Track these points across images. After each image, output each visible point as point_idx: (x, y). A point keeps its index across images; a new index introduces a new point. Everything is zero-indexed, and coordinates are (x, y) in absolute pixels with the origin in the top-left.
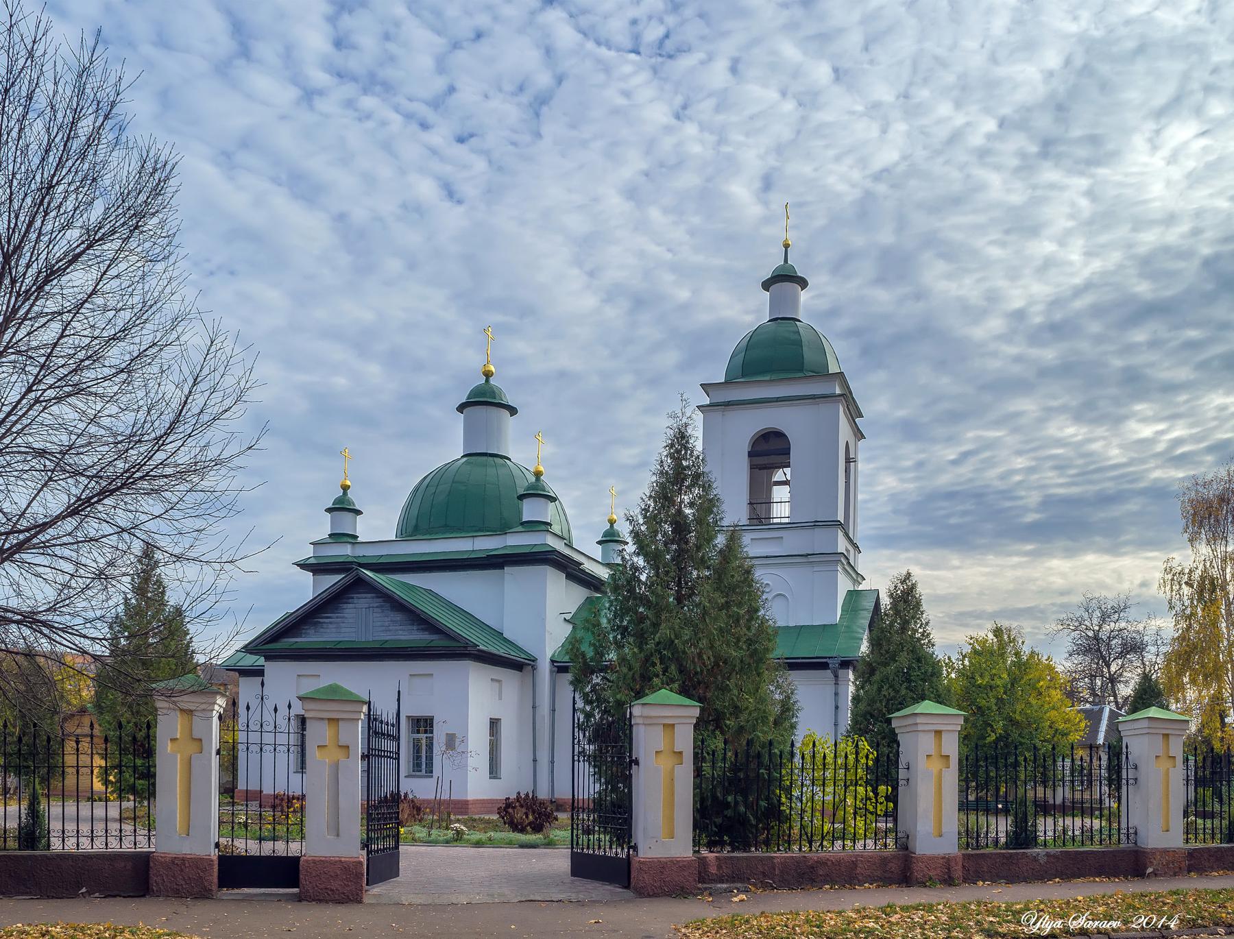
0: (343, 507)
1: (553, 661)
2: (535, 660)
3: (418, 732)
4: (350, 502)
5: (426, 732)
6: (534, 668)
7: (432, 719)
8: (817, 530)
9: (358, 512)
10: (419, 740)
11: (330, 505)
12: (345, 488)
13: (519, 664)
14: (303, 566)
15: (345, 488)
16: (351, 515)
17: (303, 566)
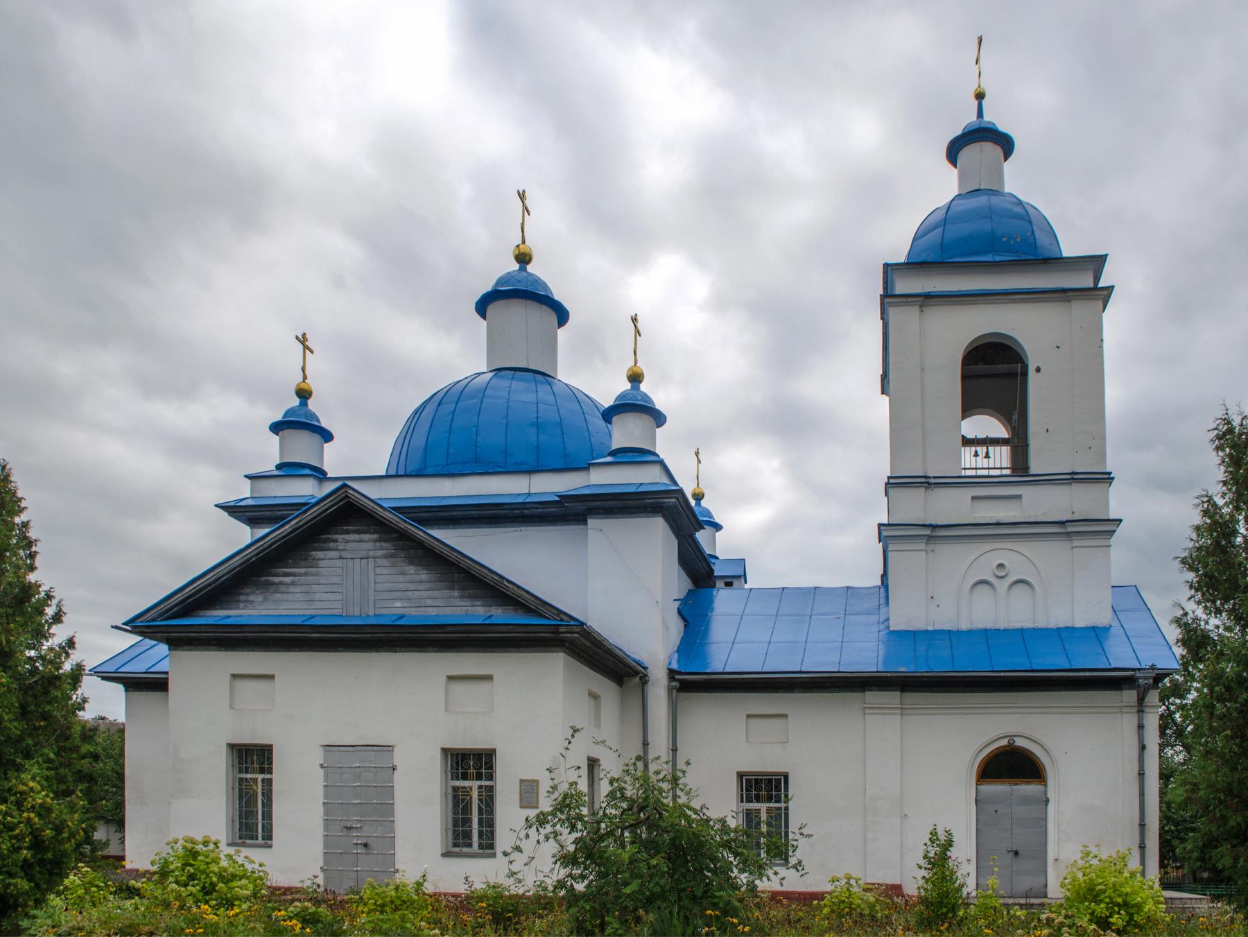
1: (672, 673)
3: (465, 777)
5: (479, 777)
6: (644, 680)
10: (467, 791)
13: (619, 670)
16: (316, 438)
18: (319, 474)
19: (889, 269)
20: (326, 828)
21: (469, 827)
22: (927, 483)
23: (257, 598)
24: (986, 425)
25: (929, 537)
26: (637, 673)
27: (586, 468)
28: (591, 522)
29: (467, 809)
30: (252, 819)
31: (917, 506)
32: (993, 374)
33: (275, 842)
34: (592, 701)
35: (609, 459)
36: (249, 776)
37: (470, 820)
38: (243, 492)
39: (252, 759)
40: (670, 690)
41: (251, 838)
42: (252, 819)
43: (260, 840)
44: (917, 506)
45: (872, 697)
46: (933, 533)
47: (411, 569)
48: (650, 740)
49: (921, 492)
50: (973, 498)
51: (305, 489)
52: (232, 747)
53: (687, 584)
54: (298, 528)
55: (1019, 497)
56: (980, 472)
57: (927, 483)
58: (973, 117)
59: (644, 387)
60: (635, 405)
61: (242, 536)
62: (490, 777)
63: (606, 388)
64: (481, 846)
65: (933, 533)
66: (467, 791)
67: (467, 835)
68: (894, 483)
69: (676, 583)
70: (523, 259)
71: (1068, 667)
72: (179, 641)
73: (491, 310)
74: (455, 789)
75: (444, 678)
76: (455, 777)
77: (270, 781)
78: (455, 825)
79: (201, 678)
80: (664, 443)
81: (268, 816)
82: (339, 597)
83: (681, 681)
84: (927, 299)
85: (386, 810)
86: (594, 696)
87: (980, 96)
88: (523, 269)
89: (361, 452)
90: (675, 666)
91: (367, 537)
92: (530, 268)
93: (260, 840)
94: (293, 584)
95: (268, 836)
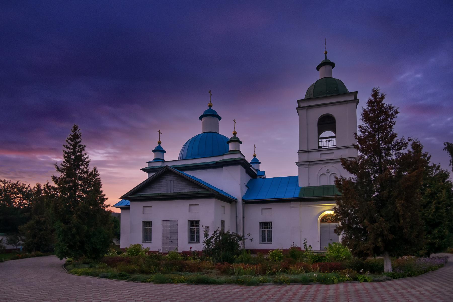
1: (243, 200)
2: (237, 199)
3: (193, 226)
5: (196, 226)
7: (199, 221)
10: (194, 229)
13: (230, 200)
18: (163, 161)
20: (163, 238)
21: (193, 237)
22: (308, 151)
25: (309, 165)
27: (223, 155)
29: (194, 233)
30: (147, 237)
31: (305, 157)
34: (223, 208)
37: (194, 235)
38: (146, 165)
39: (147, 224)
40: (243, 204)
42: (147, 237)
45: (293, 203)
46: (310, 163)
47: (181, 182)
48: (238, 215)
50: (321, 154)
51: (159, 164)
52: (143, 222)
55: (333, 153)
58: (324, 59)
59: (236, 136)
61: (145, 176)
62: (199, 226)
65: (310, 163)
66: (194, 229)
67: (194, 239)
69: (248, 178)
72: (132, 200)
74: (191, 229)
77: (151, 229)
78: (191, 236)
81: (151, 236)
84: (309, 107)
87: (326, 53)
88: (210, 108)
95: (151, 240)
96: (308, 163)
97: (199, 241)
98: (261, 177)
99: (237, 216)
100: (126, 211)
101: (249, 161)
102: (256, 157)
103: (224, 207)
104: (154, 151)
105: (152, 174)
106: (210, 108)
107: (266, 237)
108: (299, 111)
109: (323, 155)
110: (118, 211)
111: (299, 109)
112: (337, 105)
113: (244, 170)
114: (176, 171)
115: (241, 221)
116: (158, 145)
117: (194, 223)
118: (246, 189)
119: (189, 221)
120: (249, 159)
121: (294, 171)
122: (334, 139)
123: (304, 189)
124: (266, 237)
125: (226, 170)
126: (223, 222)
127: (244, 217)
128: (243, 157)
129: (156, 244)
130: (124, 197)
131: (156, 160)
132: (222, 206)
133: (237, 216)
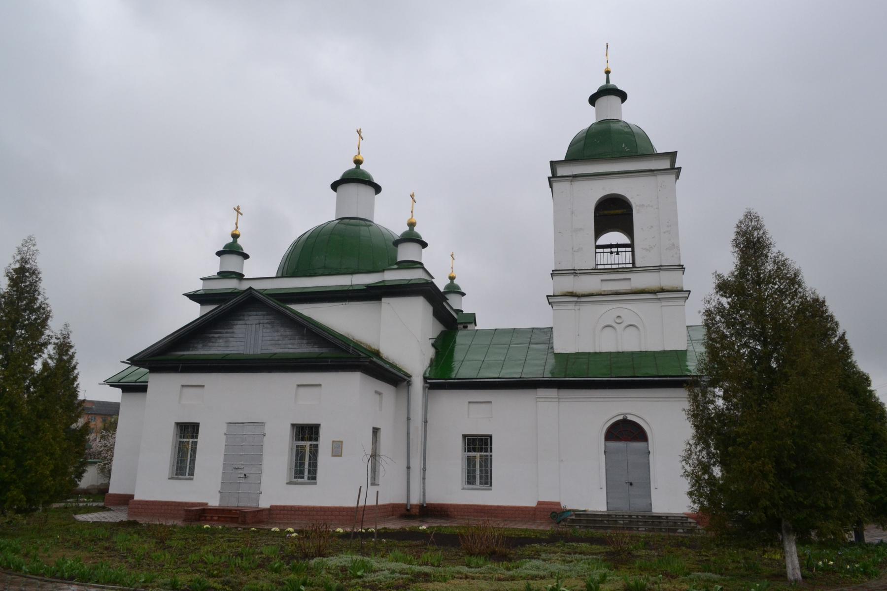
0: (232, 250)
1: (425, 379)
2: (410, 376)
3: (303, 440)
4: (240, 247)
5: (310, 440)
6: (409, 384)
8: (662, 273)
9: (246, 256)
10: (303, 447)
11: (221, 249)
12: (235, 236)
14: (194, 297)
15: (235, 236)
16: (240, 258)
17: (194, 297)
18: (240, 276)
19: (553, 164)
20: (224, 469)
21: (304, 467)
22: (575, 272)
23: (201, 346)
24: (615, 237)
26: (405, 380)
27: (383, 271)
28: (383, 299)
32: (614, 214)
33: (195, 477)
34: (377, 396)
35: (396, 266)
36: (185, 440)
38: (198, 286)
40: (424, 388)
41: (182, 474)
43: (187, 476)
44: (569, 284)
49: (572, 277)
51: (230, 284)
52: (177, 424)
53: (439, 328)
54: (226, 303)
56: (606, 267)
57: (575, 272)
60: (412, 238)
61: (194, 312)
63: (399, 229)
64: (309, 479)
66: (303, 447)
68: (555, 273)
70: (358, 162)
71: (655, 373)
73: (340, 189)
75: (295, 386)
76: (297, 439)
77: (196, 443)
79: (164, 387)
80: (426, 257)
82: (243, 344)
83: (430, 383)
85: (258, 458)
86: (378, 393)
89: (262, 268)
90: (427, 375)
91: (260, 313)
92: (362, 167)
93: (187, 476)
94: (219, 338)
95: (192, 473)
96: (575, 299)
97: (315, 478)
98: (466, 327)
99: (409, 419)
100: (135, 398)
101: (442, 289)
102: (455, 281)
103: (380, 394)
104: (219, 254)
105: (209, 308)
106: (358, 167)
107: (478, 472)
108: (554, 185)
109: (604, 283)
110: (115, 395)
111: (553, 179)
112: (631, 177)
113: (430, 309)
114: (272, 302)
115: (420, 432)
116: (231, 240)
117: (307, 433)
118: (431, 352)
119: (293, 425)
120: (441, 284)
121: (538, 316)
122: (630, 249)
123: (564, 359)
124: (478, 472)
125: (389, 304)
126: (376, 431)
127: (426, 422)
128: (427, 278)
129: (205, 489)
130: (135, 361)
131: (223, 275)
132: (376, 392)
133: (409, 419)
